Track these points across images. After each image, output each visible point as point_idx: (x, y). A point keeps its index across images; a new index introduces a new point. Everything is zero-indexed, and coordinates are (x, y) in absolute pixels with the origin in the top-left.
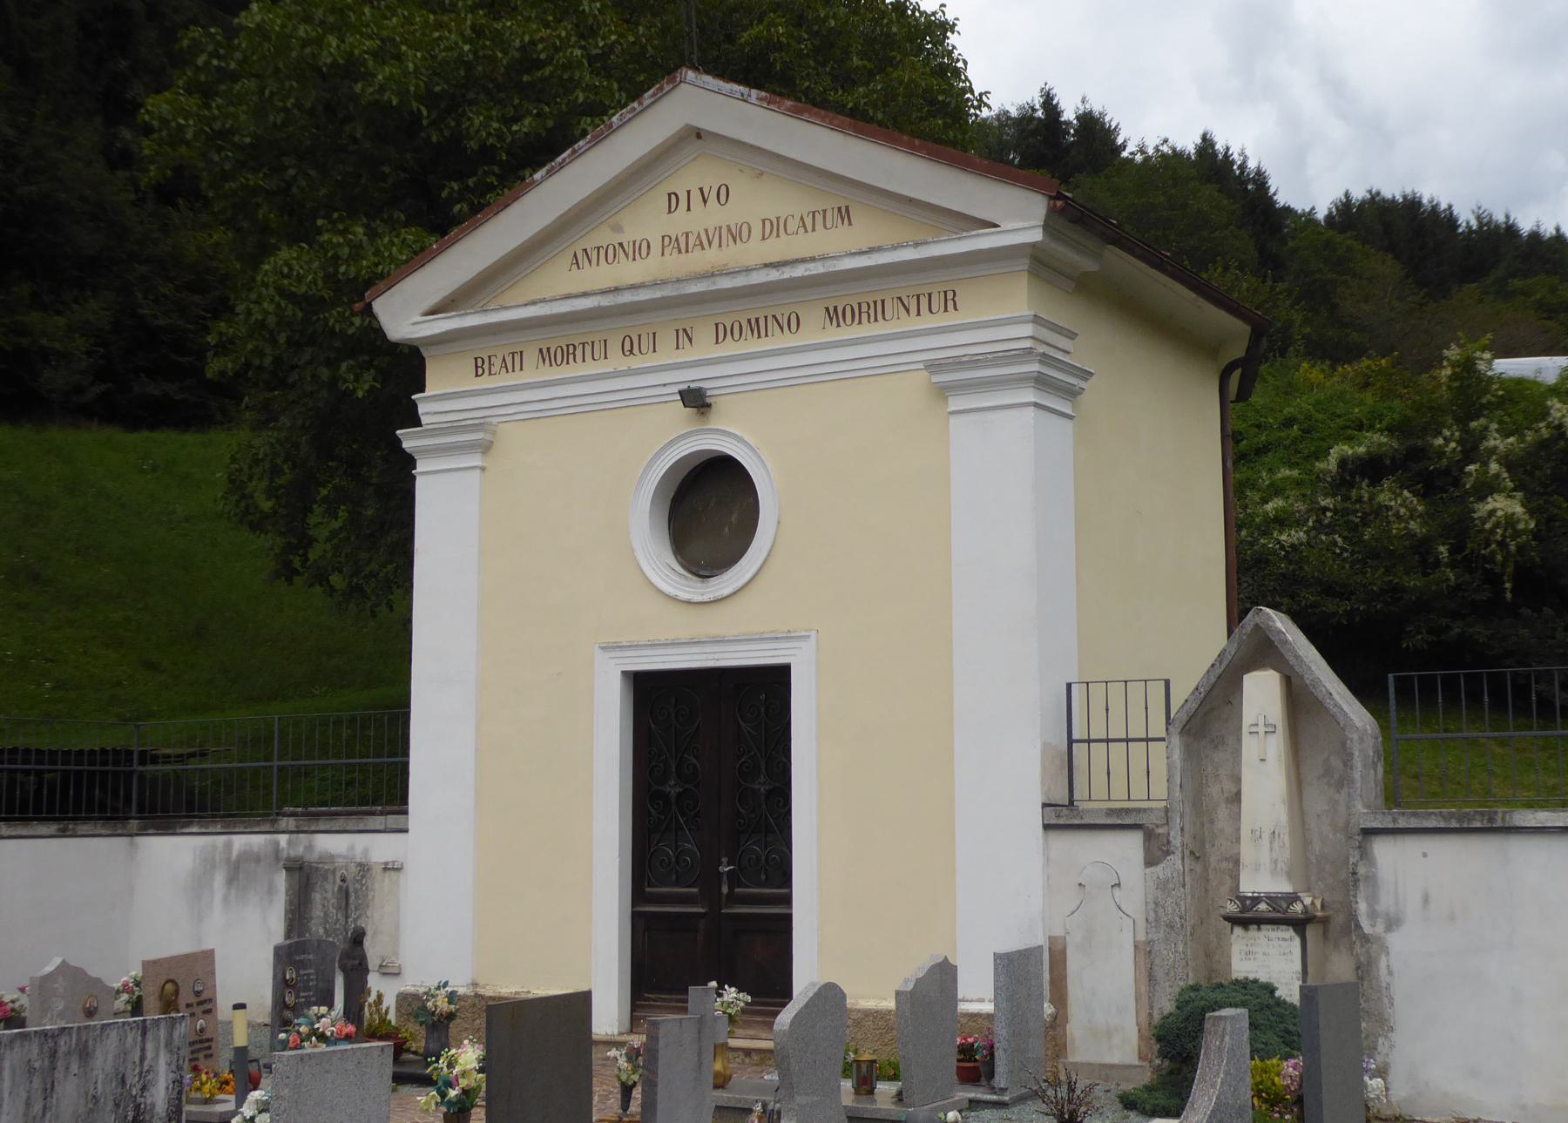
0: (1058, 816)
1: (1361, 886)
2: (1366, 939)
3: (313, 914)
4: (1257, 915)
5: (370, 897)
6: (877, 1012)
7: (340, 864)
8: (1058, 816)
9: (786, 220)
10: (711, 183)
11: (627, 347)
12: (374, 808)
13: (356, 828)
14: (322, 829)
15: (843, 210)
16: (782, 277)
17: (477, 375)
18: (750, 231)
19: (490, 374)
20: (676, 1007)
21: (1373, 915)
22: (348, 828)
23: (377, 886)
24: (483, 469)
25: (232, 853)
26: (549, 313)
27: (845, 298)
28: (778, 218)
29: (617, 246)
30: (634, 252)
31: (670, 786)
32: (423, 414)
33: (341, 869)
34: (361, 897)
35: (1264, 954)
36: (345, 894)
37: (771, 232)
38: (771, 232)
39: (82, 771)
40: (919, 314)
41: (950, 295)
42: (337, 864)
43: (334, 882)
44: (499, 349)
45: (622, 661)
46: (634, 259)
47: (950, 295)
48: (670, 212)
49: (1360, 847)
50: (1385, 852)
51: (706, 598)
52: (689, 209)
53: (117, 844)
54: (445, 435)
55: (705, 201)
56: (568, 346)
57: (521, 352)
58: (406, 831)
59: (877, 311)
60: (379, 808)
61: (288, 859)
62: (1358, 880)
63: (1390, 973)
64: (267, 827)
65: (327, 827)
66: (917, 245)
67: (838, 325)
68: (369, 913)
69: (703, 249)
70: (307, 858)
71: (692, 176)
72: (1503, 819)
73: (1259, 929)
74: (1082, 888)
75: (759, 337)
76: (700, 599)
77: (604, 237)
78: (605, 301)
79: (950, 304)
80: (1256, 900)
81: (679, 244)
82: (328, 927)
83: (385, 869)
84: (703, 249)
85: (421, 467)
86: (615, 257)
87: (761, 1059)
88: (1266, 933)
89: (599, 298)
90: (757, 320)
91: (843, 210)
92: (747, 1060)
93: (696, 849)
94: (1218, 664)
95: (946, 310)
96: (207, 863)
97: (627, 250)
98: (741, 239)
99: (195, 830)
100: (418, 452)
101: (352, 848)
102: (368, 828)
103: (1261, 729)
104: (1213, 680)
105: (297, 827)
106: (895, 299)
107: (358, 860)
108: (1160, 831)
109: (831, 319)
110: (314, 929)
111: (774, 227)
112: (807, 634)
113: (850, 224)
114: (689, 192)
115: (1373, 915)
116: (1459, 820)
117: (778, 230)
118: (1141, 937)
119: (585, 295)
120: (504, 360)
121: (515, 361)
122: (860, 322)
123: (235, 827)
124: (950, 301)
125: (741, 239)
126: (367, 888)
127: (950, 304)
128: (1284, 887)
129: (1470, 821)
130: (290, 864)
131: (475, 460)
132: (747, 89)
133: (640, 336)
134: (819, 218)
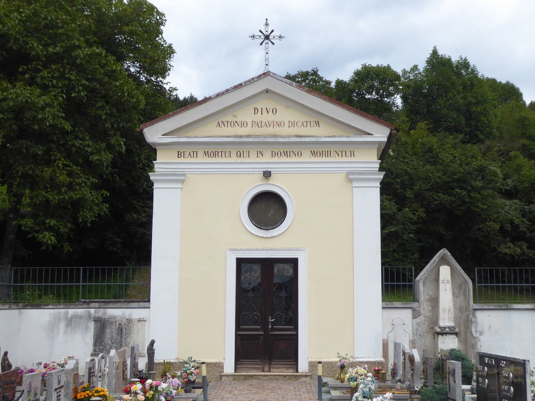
0: (387, 305)
1: (473, 324)
2: (474, 338)
3: (106, 337)
4: (446, 332)
5: (132, 330)
6: (329, 362)
7: (119, 319)
8: (387, 305)
9: (297, 123)
10: (270, 106)
11: (239, 154)
12: (120, 300)
13: (126, 307)
14: (110, 307)
15: (317, 122)
16: (301, 141)
17: (178, 157)
18: (284, 124)
19: (184, 157)
20: (258, 364)
21: (476, 331)
22: (122, 307)
23: (135, 327)
24: (181, 188)
25: (68, 315)
26: (214, 141)
27: (320, 149)
28: (294, 121)
29: (235, 122)
30: (241, 125)
31: (250, 294)
32: (156, 168)
33: (119, 321)
34: (128, 330)
35: (448, 342)
36: (120, 330)
37: (292, 125)
38: (292, 125)
39: (48, 286)
40: (342, 156)
41: (352, 152)
42: (117, 319)
43: (116, 325)
44: (188, 150)
45: (236, 254)
46: (241, 127)
47: (352, 152)
48: (255, 114)
49: (473, 314)
50: (479, 314)
51: (268, 236)
52: (262, 114)
53: (14, 313)
54: (169, 176)
55: (268, 112)
56: (215, 152)
57: (197, 152)
58: (150, 308)
59: (328, 154)
60: (123, 300)
61: (95, 317)
62: (472, 322)
63: (481, 347)
64: (85, 306)
65: (113, 306)
66: (347, 137)
67: (315, 157)
68: (131, 336)
69: (267, 127)
70: (104, 317)
71: (263, 104)
72: (510, 306)
73: (446, 336)
74: (393, 325)
75: (287, 157)
76: (266, 236)
77: (230, 118)
78: (236, 140)
79: (352, 155)
80: (445, 328)
81: (259, 125)
82: (113, 341)
83: (139, 321)
84: (267, 127)
85: (155, 186)
86: (234, 125)
87: (290, 378)
88: (448, 337)
89: (234, 138)
90: (287, 152)
91: (317, 122)
92: (284, 379)
93: (259, 314)
94: (433, 264)
95: (351, 156)
96: (57, 319)
97: (239, 124)
98: (281, 126)
99: (50, 307)
100: (154, 181)
101: (124, 314)
102: (131, 307)
103: (445, 282)
104: (432, 267)
105: (99, 306)
106: (334, 151)
107: (127, 318)
108: (417, 309)
109: (313, 155)
110: (106, 342)
111: (293, 124)
112: (305, 249)
113: (319, 127)
114: (262, 109)
115: (476, 331)
116: (499, 307)
117: (294, 125)
118: (411, 339)
119: (229, 137)
120: (190, 153)
121: (195, 154)
122: (322, 157)
123: (57, 306)
124: (352, 154)
125: (281, 126)
126: (131, 327)
127: (352, 155)
128: (452, 324)
129: (502, 307)
130: (96, 319)
131: (179, 185)
132: (292, 82)
133: (243, 152)
134: (309, 124)
